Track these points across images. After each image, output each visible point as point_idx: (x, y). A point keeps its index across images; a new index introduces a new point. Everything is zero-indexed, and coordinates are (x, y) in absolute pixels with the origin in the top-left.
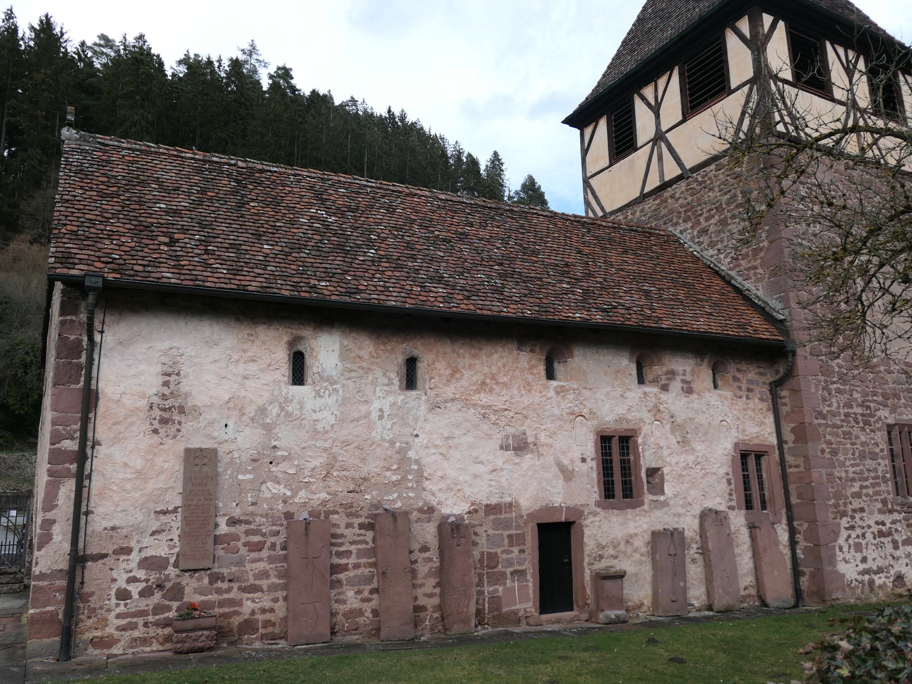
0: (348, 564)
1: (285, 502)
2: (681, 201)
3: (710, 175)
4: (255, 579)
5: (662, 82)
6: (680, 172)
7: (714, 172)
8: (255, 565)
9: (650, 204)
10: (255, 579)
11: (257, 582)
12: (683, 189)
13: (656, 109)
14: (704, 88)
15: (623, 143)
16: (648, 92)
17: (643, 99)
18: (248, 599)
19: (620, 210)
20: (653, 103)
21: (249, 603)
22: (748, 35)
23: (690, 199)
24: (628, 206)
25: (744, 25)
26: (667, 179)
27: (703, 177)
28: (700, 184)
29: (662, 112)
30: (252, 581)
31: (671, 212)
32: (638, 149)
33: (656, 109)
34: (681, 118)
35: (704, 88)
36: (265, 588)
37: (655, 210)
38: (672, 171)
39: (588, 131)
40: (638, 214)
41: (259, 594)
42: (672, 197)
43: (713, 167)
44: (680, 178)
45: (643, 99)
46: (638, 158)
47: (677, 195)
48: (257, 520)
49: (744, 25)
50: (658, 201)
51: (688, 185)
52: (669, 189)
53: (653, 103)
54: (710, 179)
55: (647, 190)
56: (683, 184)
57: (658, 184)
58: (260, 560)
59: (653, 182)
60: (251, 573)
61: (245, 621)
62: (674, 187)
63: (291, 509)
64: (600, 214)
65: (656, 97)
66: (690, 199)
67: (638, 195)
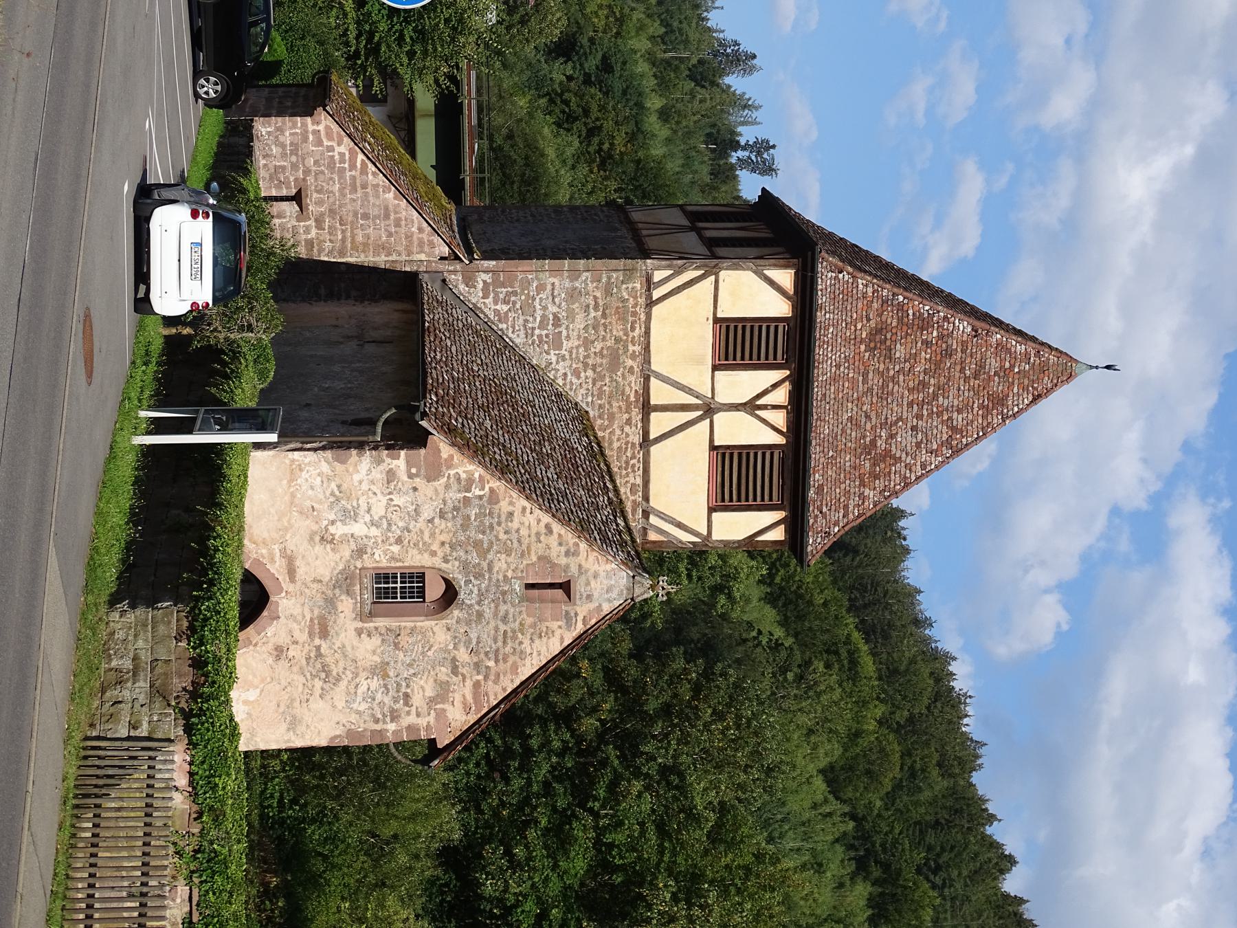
2: (618, 432)
3: (631, 475)
5: (779, 419)
6: (652, 437)
7: (632, 480)
9: (633, 384)
12: (630, 439)
13: (751, 406)
14: (735, 478)
15: (738, 342)
16: (781, 396)
17: (775, 386)
19: (647, 333)
20: (758, 403)
22: (759, 539)
23: (616, 445)
24: (647, 348)
25: (778, 534)
26: (653, 416)
27: (633, 466)
28: (627, 463)
29: (741, 416)
31: (612, 417)
32: (715, 368)
33: (751, 406)
34: (716, 443)
35: (735, 478)
37: (623, 394)
38: (660, 423)
39: (785, 277)
40: (630, 363)
42: (629, 422)
43: (639, 481)
44: (646, 433)
45: (775, 386)
46: (699, 377)
47: (627, 429)
49: (778, 534)
50: (632, 399)
51: (633, 444)
52: (640, 416)
53: (758, 403)
54: (627, 475)
55: (654, 382)
56: (636, 439)
57: (652, 403)
59: (660, 393)
62: (640, 425)
64: (656, 294)
65: (764, 407)
66: (616, 445)
67: (653, 367)
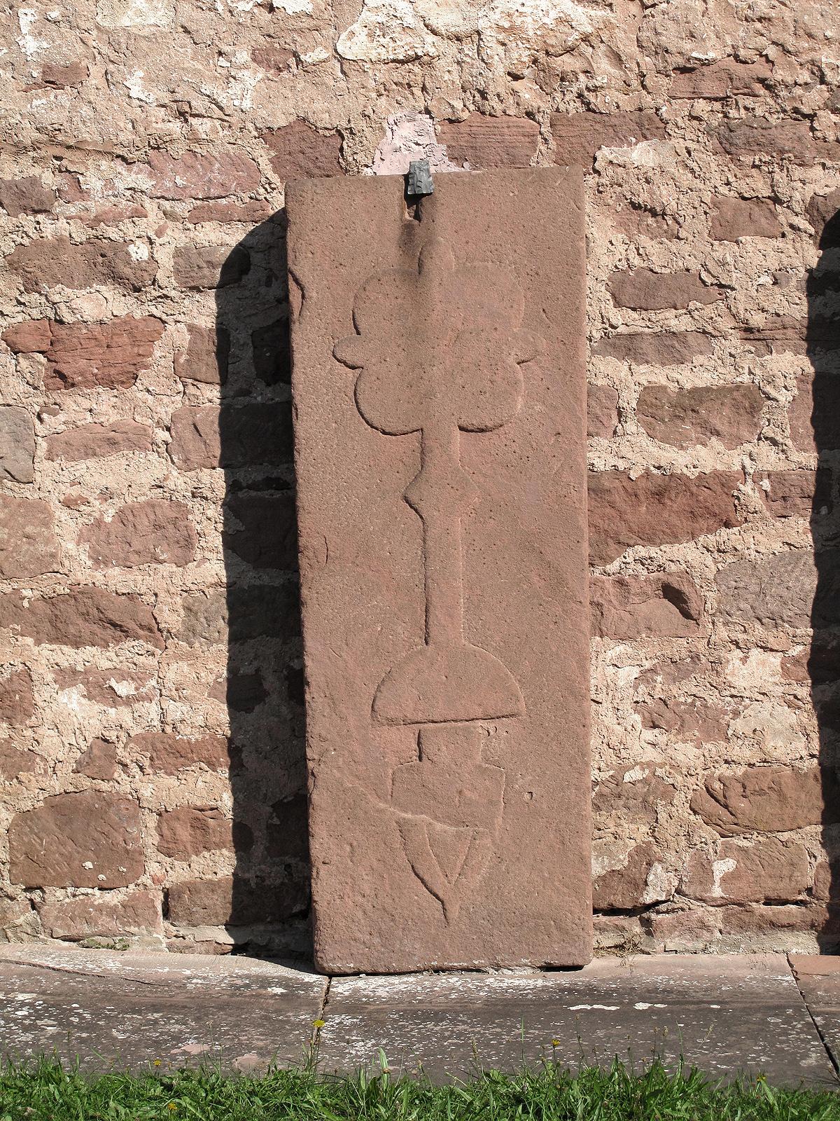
0: (724, 482)
1: (278, 57)
4: (99, 560)
8: (95, 473)
10: (99, 560)
11: (115, 578)
18: (66, 677)
21: (73, 701)
30: (80, 566)
36: (171, 618)
41: (130, 651)
48: (92, 182)
58: (136, 440)
60: (67, 526)
61: (63, 808)
63: (326, 113)
